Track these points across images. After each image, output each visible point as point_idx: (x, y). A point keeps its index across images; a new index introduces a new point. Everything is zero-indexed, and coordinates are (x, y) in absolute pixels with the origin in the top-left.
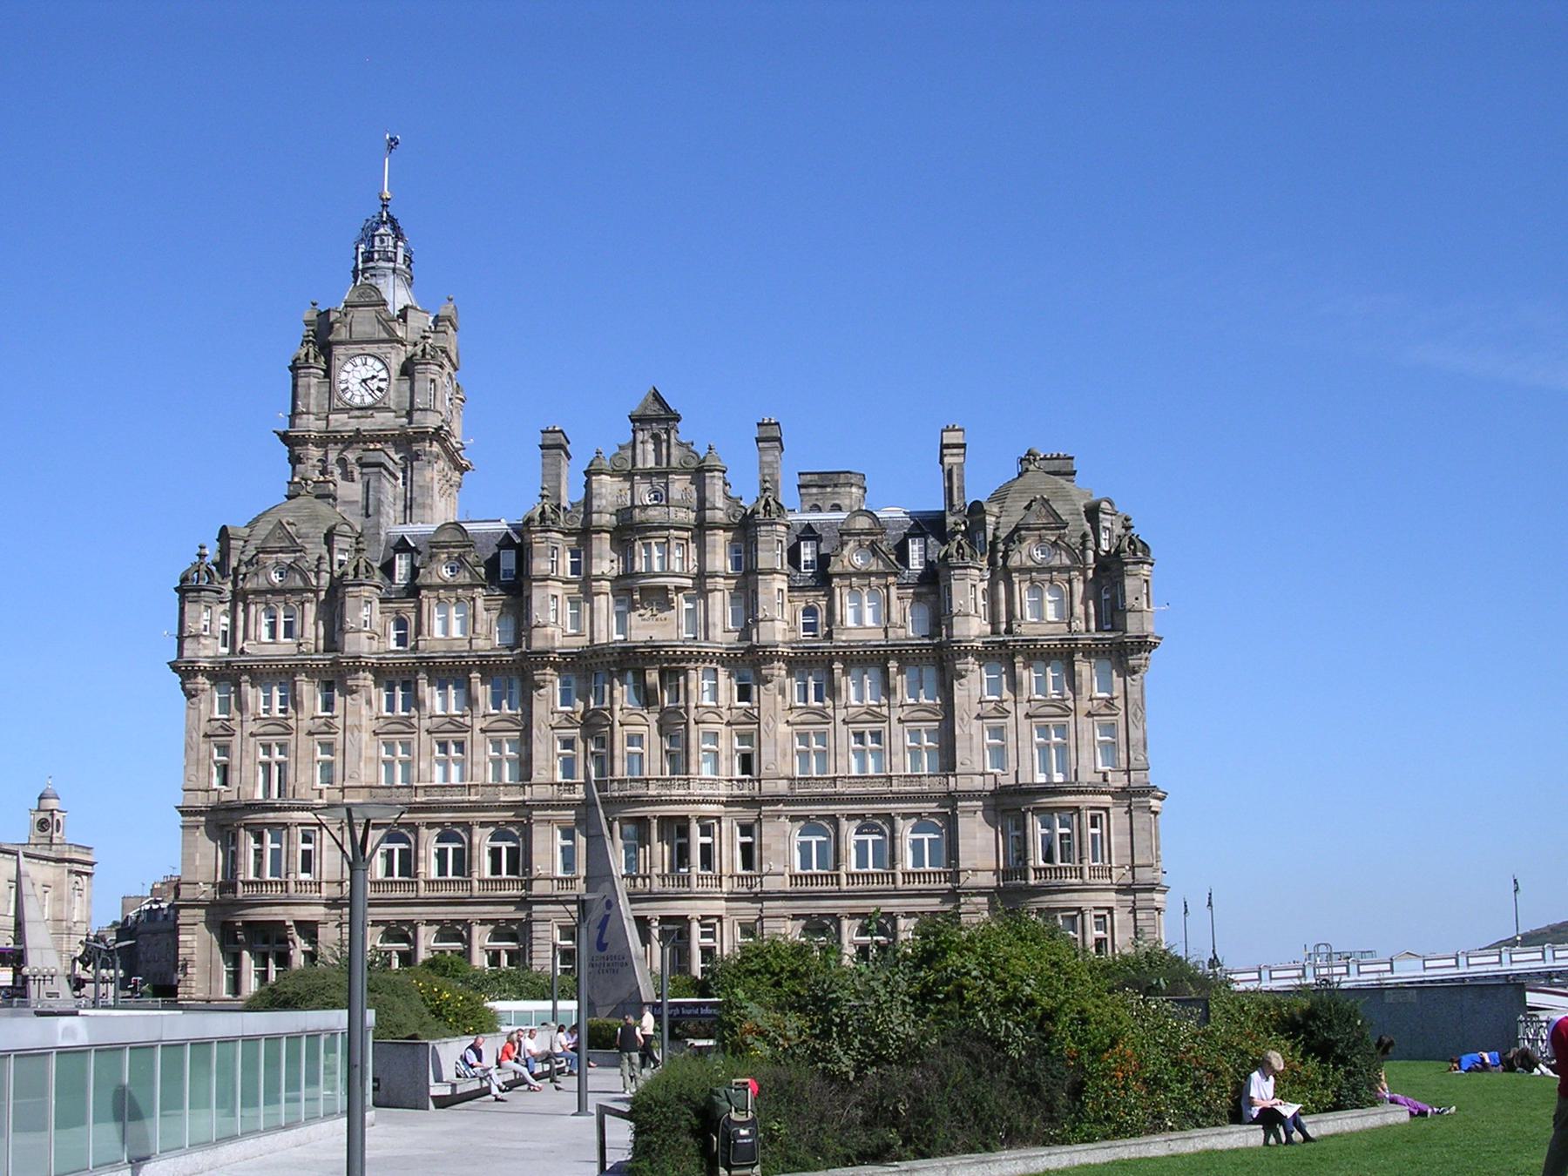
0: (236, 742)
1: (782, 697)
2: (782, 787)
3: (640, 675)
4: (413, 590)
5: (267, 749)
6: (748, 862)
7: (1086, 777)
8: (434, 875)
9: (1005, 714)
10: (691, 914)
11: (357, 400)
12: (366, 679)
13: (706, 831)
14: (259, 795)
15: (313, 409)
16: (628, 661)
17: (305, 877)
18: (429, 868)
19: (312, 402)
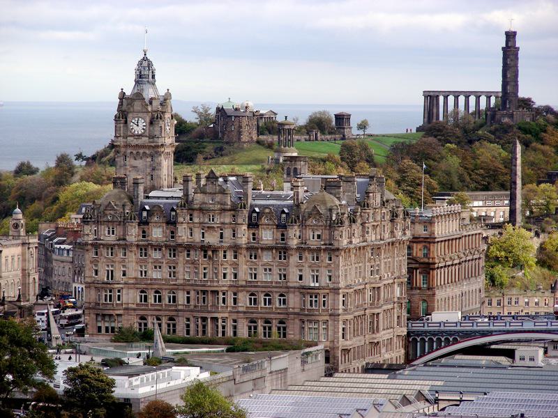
0: (99, 264)
1: (243, 258)
2: (244, 283)
3: (206, 251)
4: (147, 223)
5: (108, 266)
6: (235, 303)
7: (323, 284)
8: (153, 302)
9: (303, 266)
10: (219, 317)
11: (136, 133)
12: (134, 249)
13: (224, 294)
14: (106, 280)
15: (122, 135)
16: (205, 249)
17: (118, 302)
18: (151, 300)
19: (122, 132)
